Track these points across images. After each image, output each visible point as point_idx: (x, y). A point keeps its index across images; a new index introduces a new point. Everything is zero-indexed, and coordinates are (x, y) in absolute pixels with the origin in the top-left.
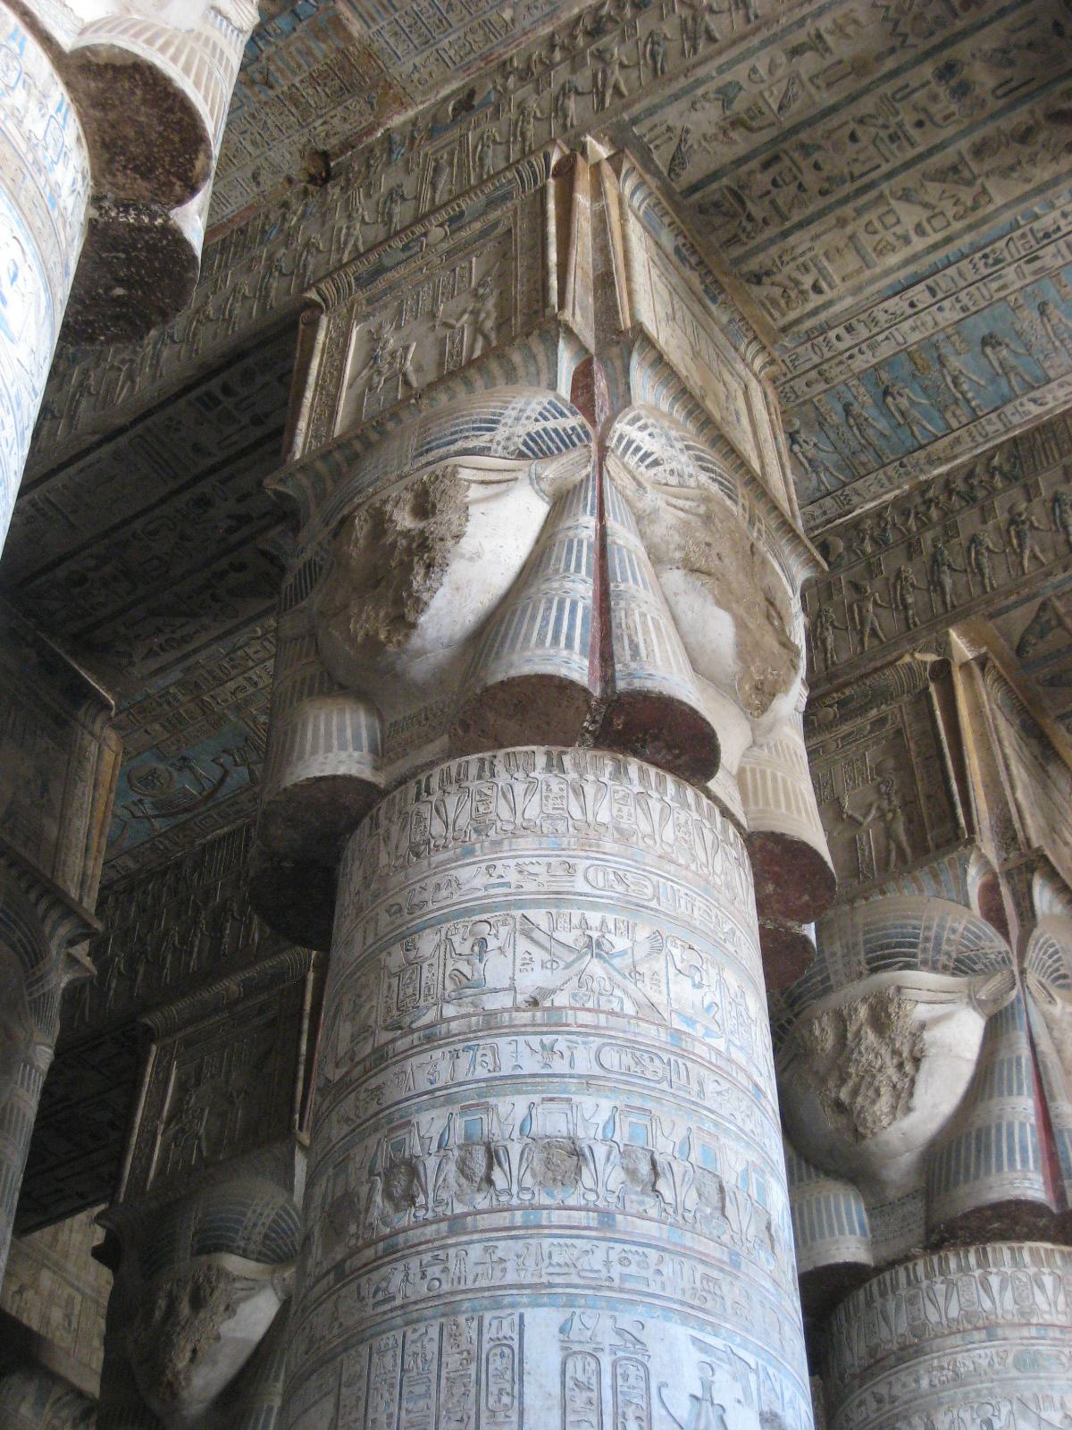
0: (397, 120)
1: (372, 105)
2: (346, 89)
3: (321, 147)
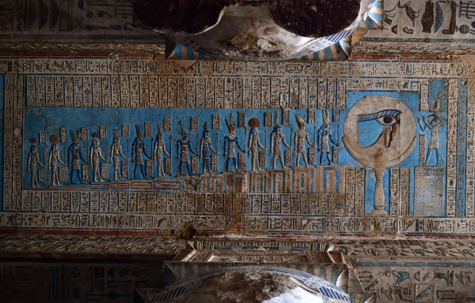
0: (232, 236)
1: (228, 223)
2: (223, 210)
3: (195, 227)
